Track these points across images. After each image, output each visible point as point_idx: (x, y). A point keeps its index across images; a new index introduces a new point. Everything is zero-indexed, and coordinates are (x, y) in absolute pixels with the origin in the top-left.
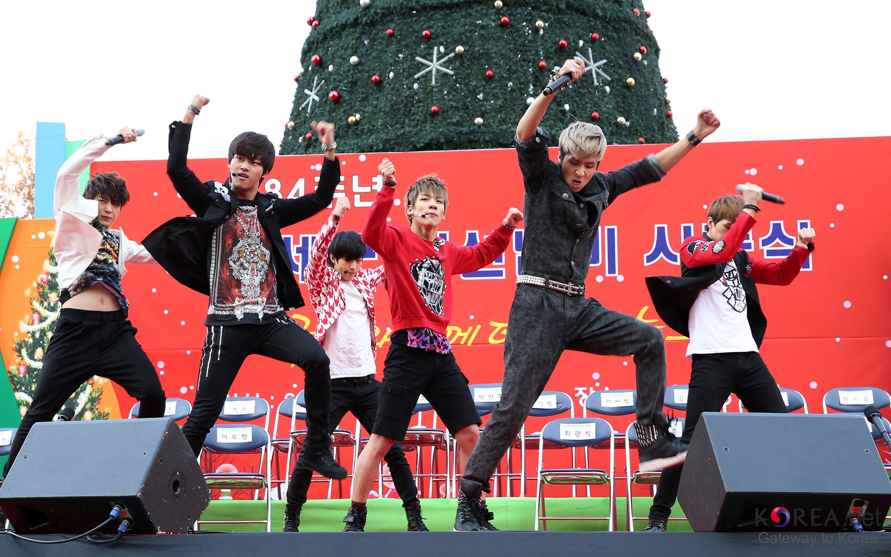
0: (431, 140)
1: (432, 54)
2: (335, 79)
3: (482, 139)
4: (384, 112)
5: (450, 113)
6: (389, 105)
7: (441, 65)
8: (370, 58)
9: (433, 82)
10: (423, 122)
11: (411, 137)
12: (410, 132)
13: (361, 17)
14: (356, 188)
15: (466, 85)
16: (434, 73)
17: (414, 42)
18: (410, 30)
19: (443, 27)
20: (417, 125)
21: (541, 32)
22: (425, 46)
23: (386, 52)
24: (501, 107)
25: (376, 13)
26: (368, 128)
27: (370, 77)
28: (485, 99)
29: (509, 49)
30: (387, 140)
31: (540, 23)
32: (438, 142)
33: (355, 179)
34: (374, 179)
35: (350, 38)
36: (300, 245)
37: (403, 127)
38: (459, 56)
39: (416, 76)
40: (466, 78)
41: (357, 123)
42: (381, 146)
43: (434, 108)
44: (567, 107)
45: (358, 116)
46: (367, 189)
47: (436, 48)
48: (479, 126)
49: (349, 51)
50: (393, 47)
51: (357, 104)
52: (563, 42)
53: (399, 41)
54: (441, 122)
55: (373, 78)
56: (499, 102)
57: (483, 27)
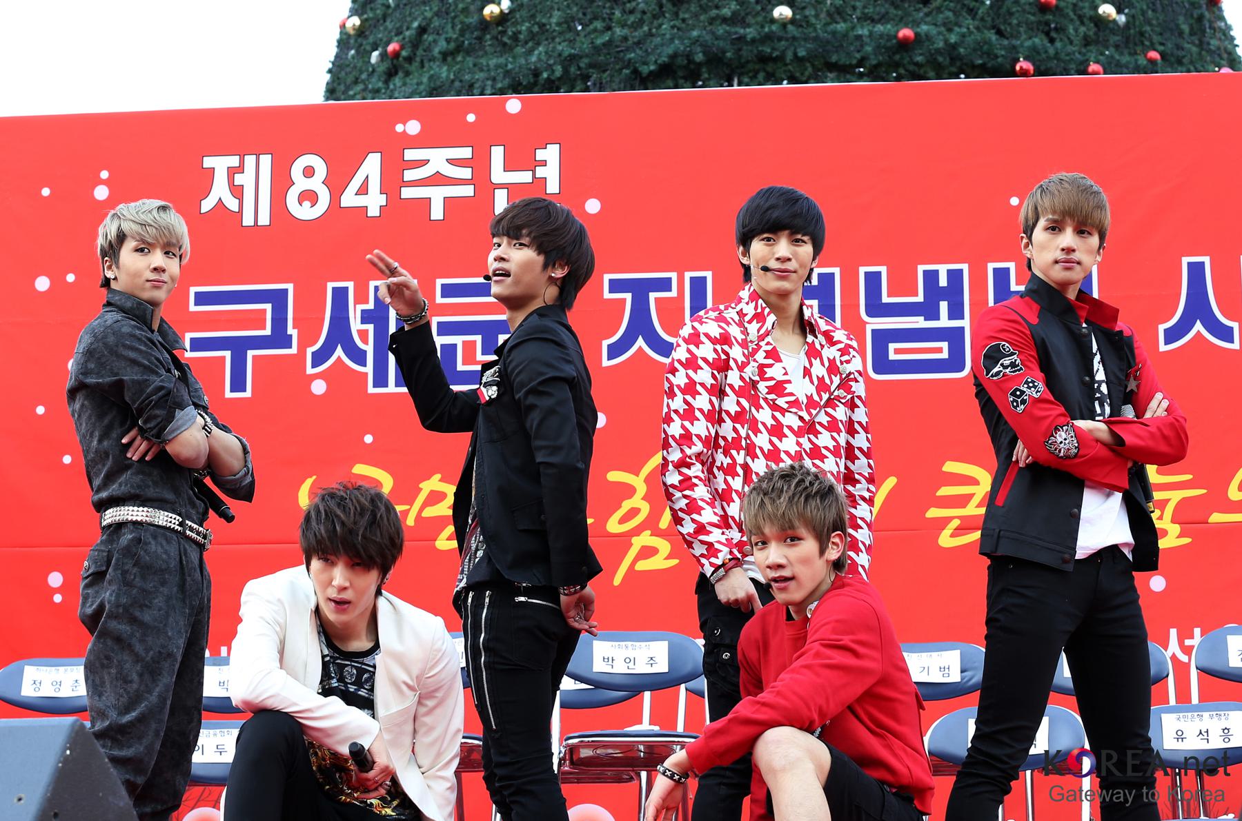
0: (674, 56)
10: (655, 17)
11: (628, 50)
12: (625, 39)
14: (498, 174)
20: (641, 23)
26: (530, 30)
30: (572, 58)
32: (690, 61)
33: (497, 153)
34: (540, 154)
36: (370, 306)
37: (609, 28)
42: (559, 71)
46: (525, 177)
48: (784, 24)
54: (696, 16)
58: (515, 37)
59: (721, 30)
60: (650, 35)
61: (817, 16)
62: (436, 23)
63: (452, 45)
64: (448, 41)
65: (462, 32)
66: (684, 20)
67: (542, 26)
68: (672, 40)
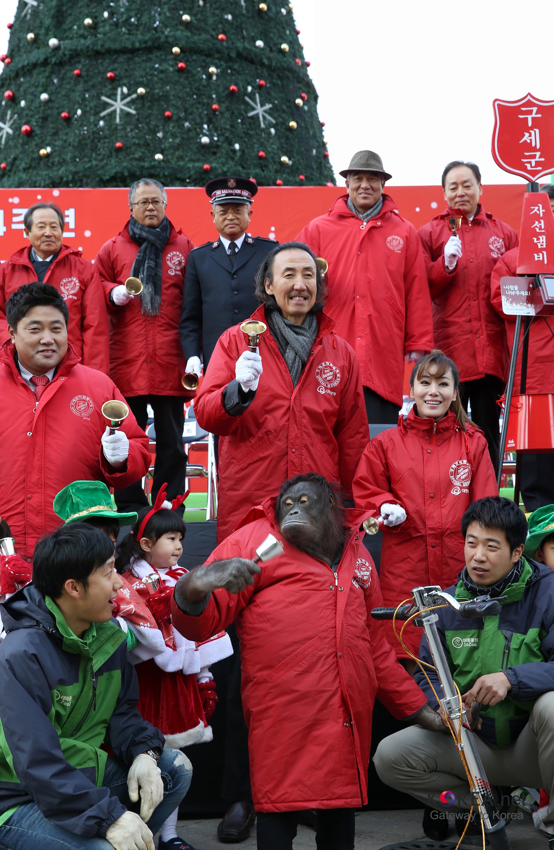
0: (116, 173)
1: (115, 95)
2: (27, 115)
3: (161, 175)
4: (73, 146)
5: (133, 149)
6: (77, 140)
7: (124, 105)
8: (59, 96)
9: (118, 120)
10: (109, 157)
11: (98, 170)
12: (97, 165)
13: (51, 57)
15: (147, 124)
16: (118, 111)
17: (100, 83)
18: (96, 71)
19: (126, 70)
21: (214, 78)
22: (110, 87)
23: (74, 91)
24: (178, 145)
25: (64, 54)
27: (59, 114)
28: (165, 137)
29: (186, 93)
30: (76, 173)
31: (212, 69)
35: (41, 76)
37: (90, 161)
38: (141, 97)
39: (103, 114)
40: (146, 118)
41: (48, 156)
42: (70, 177)
43: (118, 144)
44: (237, 146)
45: (49, 149)
47: (119, 90)
48: (159, 161)
49: (40, 89)
50: (80, 87)
51: (49, 138)
52: (233, 87)
53: (86, 82)
54: (125, 157)
55: (63, 115)
56: (178, 141)
57: (162, 72)
58: (53, 163)
59: (135, 163)
60: (107, 164)
61: (172, 159)
62: (21, 156)
63: (28, 166)
64: (26, 163)
65: (32, 160)
66: (120, 159)
67: (64, 160)
68: (115, 166)
